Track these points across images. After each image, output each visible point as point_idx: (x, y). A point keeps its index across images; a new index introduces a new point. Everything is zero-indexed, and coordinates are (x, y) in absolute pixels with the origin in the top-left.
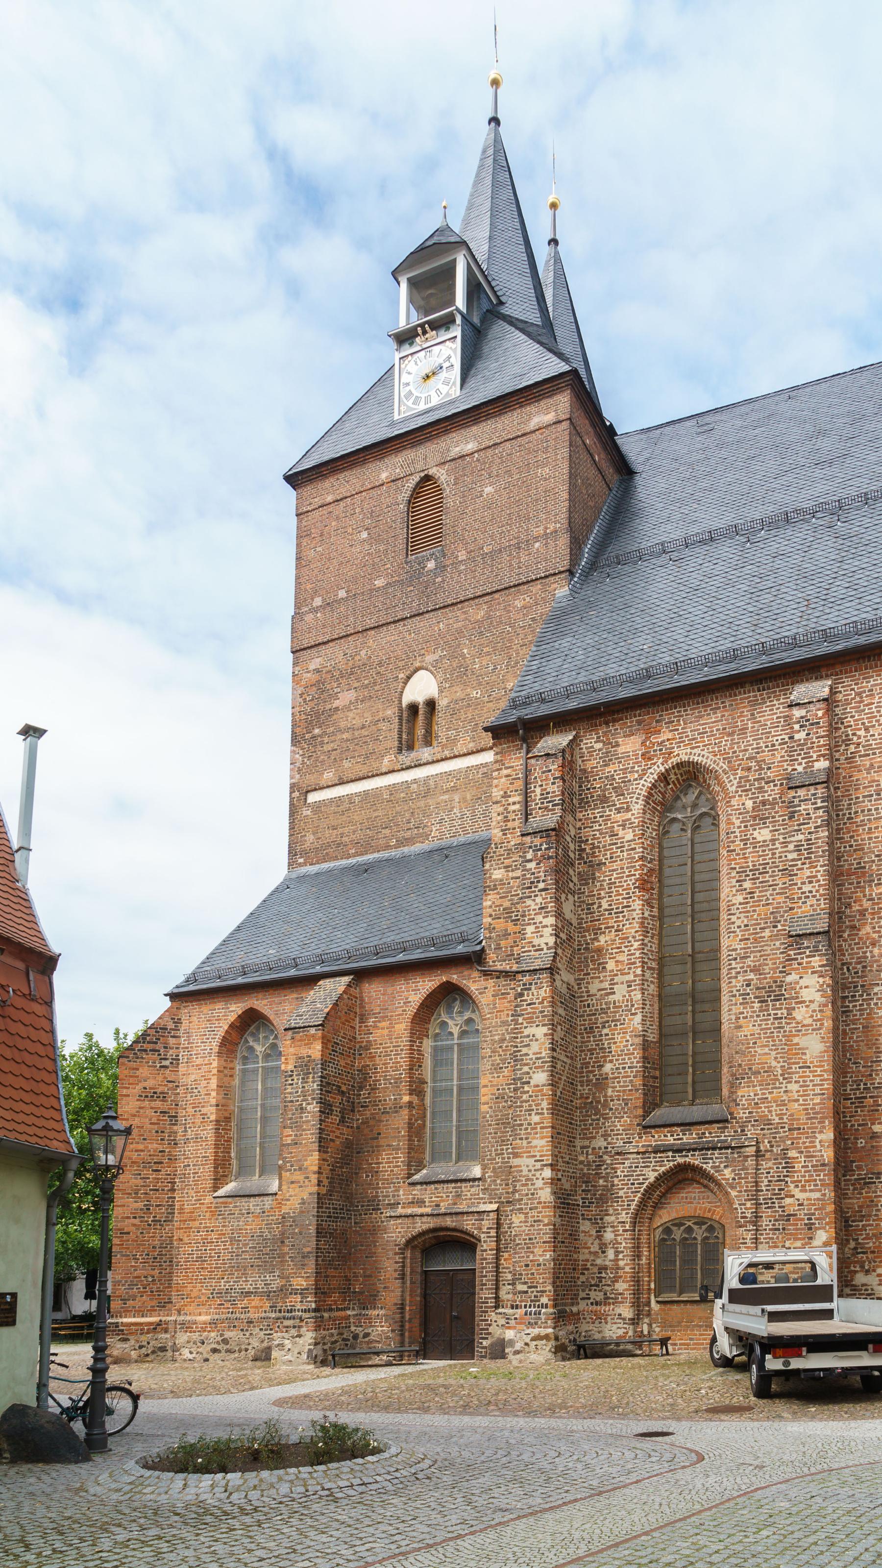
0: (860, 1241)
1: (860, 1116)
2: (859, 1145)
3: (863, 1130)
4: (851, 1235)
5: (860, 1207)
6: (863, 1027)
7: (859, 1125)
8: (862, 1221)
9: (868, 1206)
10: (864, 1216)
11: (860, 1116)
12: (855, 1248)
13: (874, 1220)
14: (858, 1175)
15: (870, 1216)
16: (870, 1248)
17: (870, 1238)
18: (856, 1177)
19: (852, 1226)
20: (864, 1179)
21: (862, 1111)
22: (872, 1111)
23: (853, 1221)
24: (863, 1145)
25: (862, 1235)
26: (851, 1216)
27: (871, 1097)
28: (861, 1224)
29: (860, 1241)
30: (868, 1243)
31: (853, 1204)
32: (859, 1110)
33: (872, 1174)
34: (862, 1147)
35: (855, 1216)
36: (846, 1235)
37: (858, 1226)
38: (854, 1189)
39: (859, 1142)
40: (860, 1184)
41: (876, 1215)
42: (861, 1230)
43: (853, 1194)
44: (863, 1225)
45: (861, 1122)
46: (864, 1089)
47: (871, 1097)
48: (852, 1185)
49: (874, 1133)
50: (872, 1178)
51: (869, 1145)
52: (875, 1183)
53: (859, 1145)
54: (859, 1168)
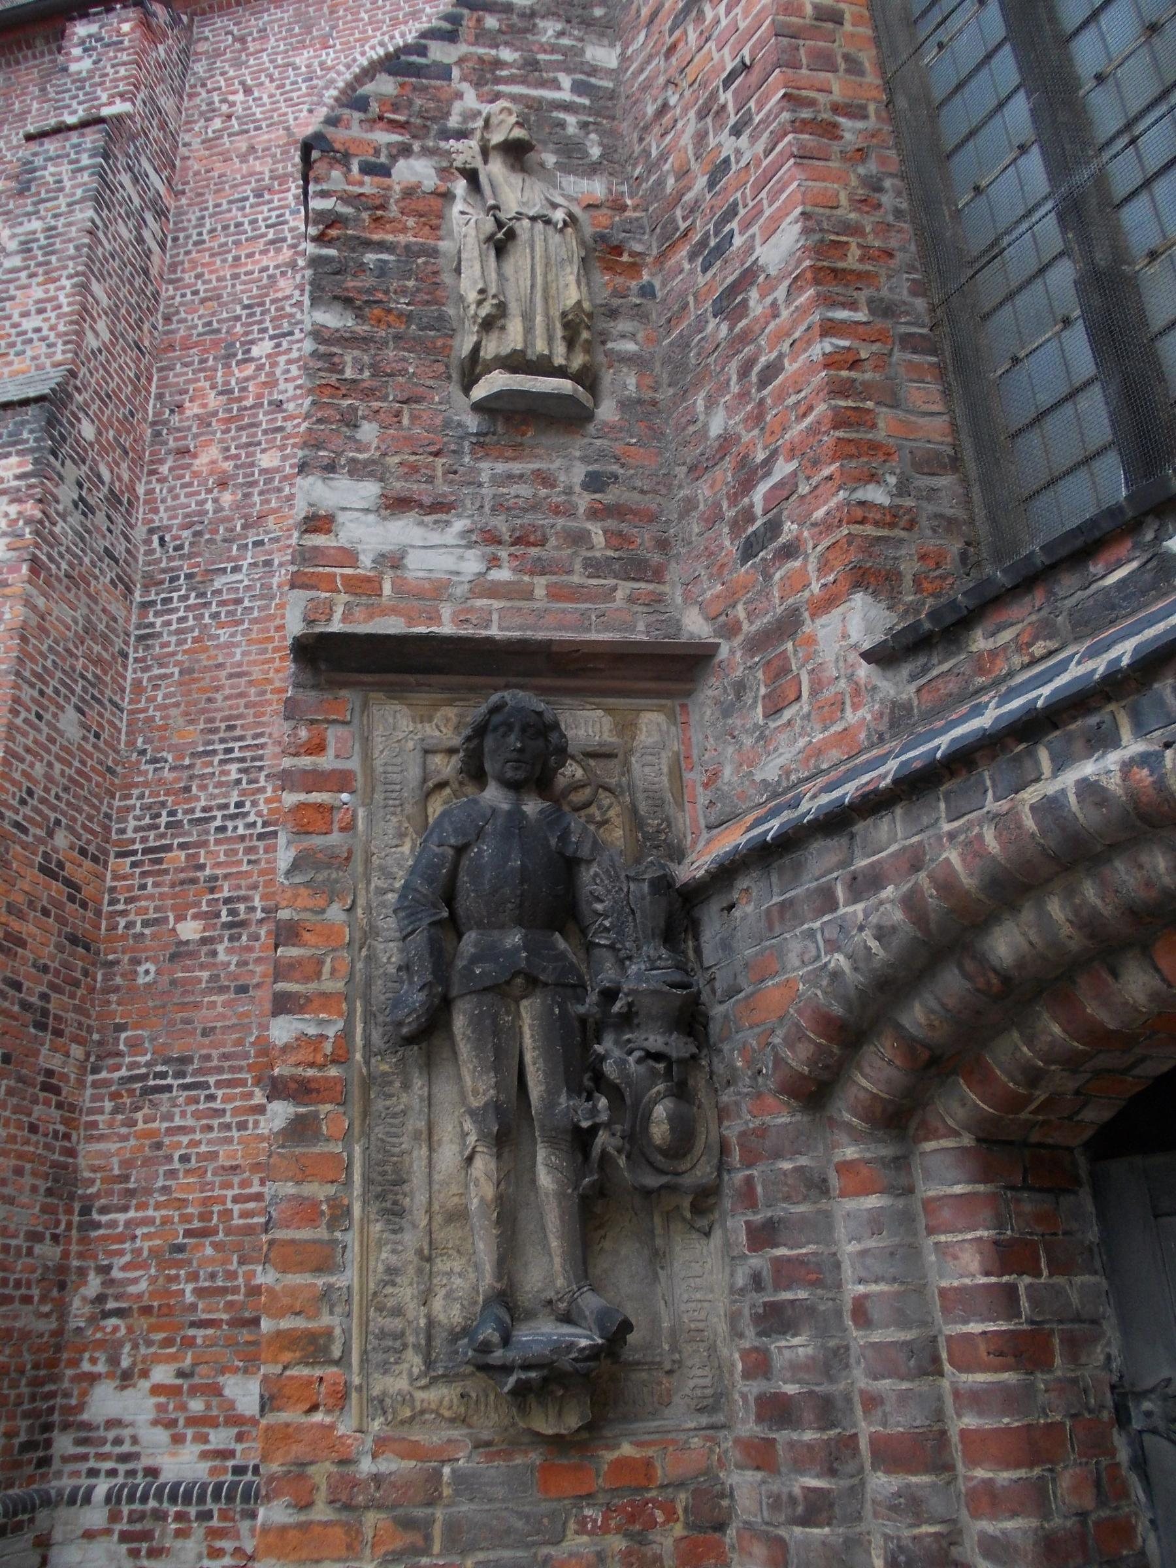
0: (116, 1274)
1: (151, 897)
2: (141, 980)
3: (154, 937)
4: (95, 1257)
5: (127, 1164)
6: (181, 672)
7: (146, 924)
8: (125, 1209)
9: (147, 1162)
10: (131, 1193)
11: (151, 897)
12: (101, 1299)
13: (158, 1207)
14: (134, 1065)
15: (148, 1191)
16: (139, 1296)
17: (144, 1266)
18: (123, 1072)
19: (98, 1225)
20: (144, 1077)
21: (156, 885)
22: (182, 883)
23: (104, 1210)
24: (148, 979)
25: (121, 1253)
26: (97, 1195)
27: (182, 846)
28: (121, 1217)
29: (116, 1274)
30: (135, 1281)
31: (108, 1155)
32: (150, 881)
33: (167, 1061)
34: (148, 985)
35: (109, 1193)
36: (81, 1255)
37: (113, 1224)
38: (116, 1111)
39: (141, 969)
40: (131, 1092)
41: (165, 1189)
42: (121, 1239)
43: (111, 1125)
44: (128, 1224)
45: (152, 915)
46: (169, 825)
47: (182, 846)
48: (115, 1096)
49: (182, 943)
50: (163, 1075)
51: (166, 978)
52: (169, 1088)
53: (141, 980)
54: (135, 1046)
